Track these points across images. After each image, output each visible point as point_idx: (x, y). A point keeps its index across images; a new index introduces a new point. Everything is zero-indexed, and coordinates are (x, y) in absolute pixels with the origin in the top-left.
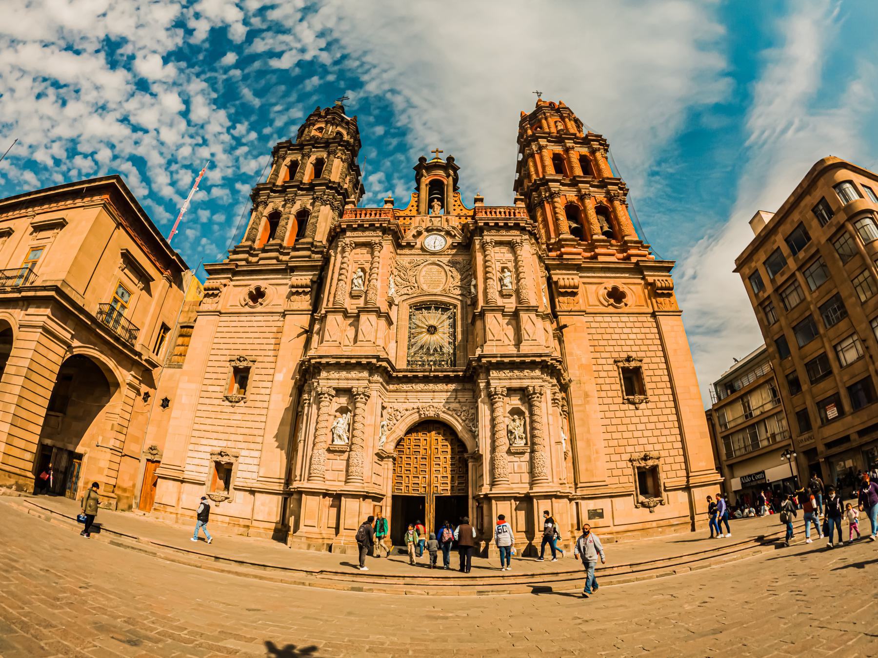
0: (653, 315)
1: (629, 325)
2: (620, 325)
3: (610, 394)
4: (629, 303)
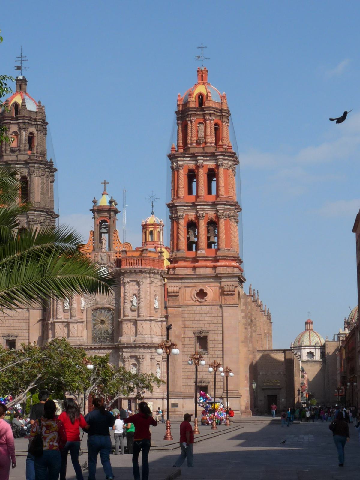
0: (221, 306)
1: (206, 312)
2: (201, 312)
3: (189, 350)
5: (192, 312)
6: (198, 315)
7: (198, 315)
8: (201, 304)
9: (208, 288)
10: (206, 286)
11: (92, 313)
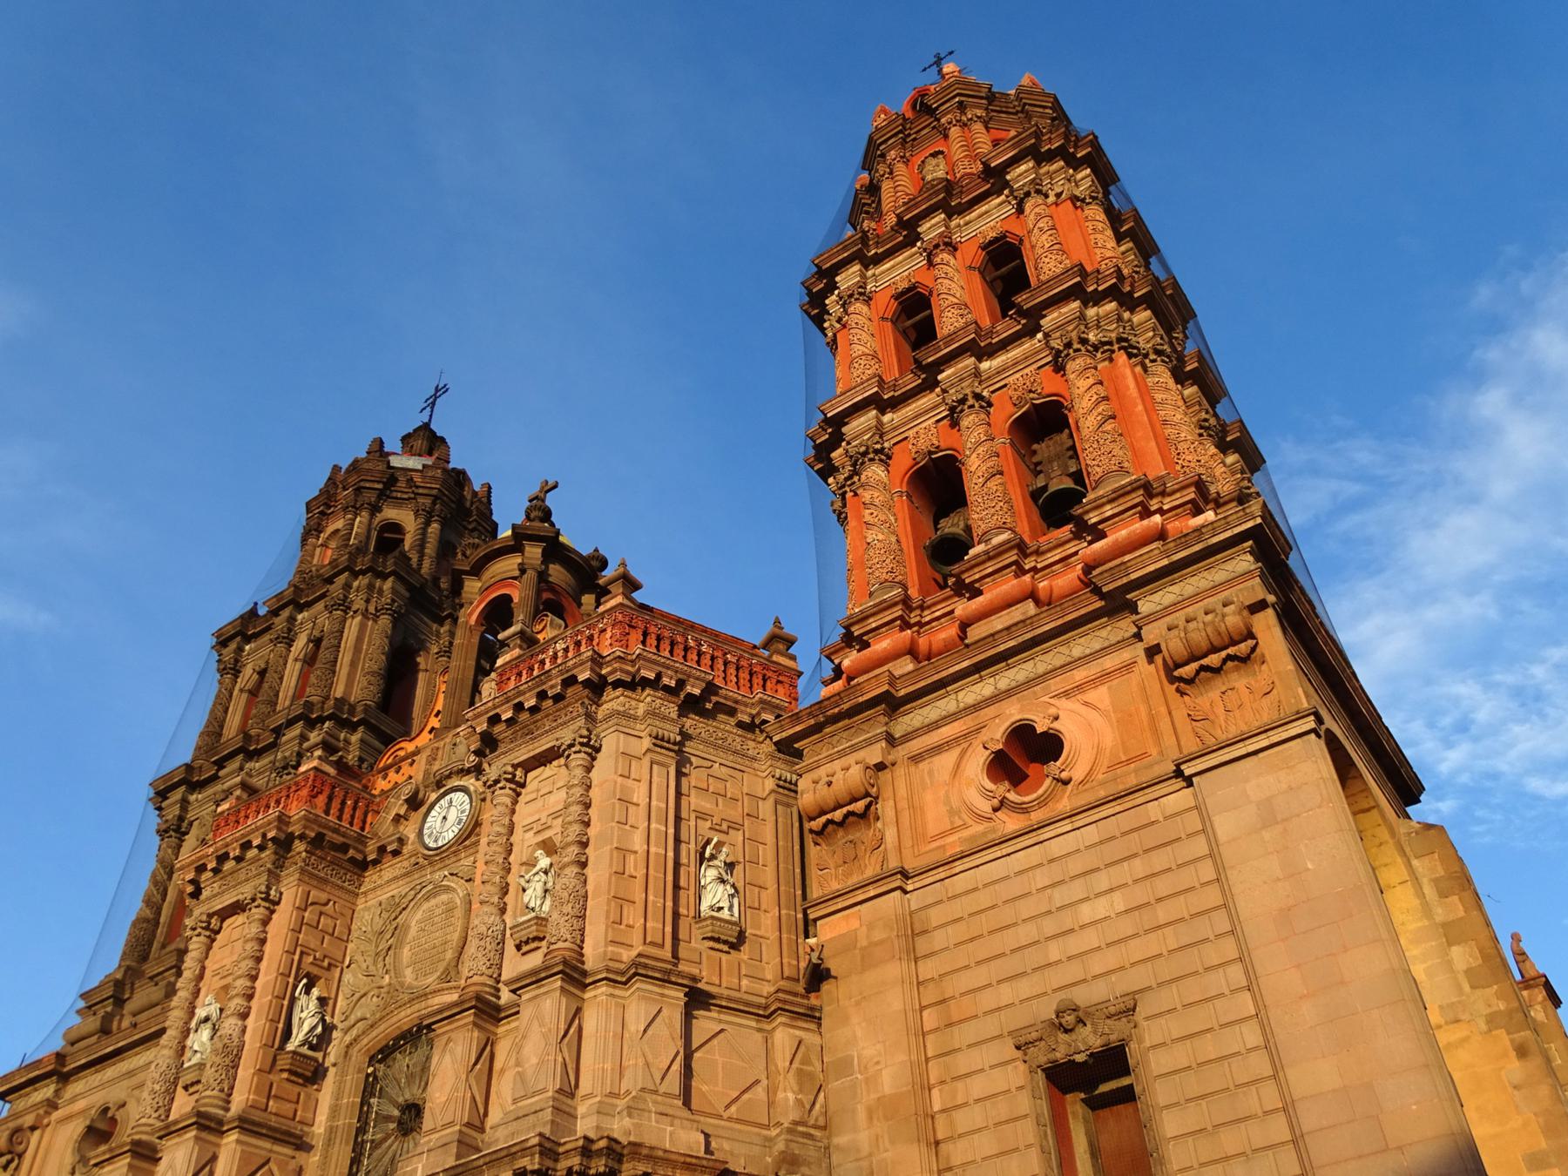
2: (1041, 878)
4: (1077, 774)
5: (983, 898)
6: (1027, 908)
7: (1027, 908)
8: (1037, 816)
9: (1063, 703)
10: (1046, 699)
11: (368, 1075)
